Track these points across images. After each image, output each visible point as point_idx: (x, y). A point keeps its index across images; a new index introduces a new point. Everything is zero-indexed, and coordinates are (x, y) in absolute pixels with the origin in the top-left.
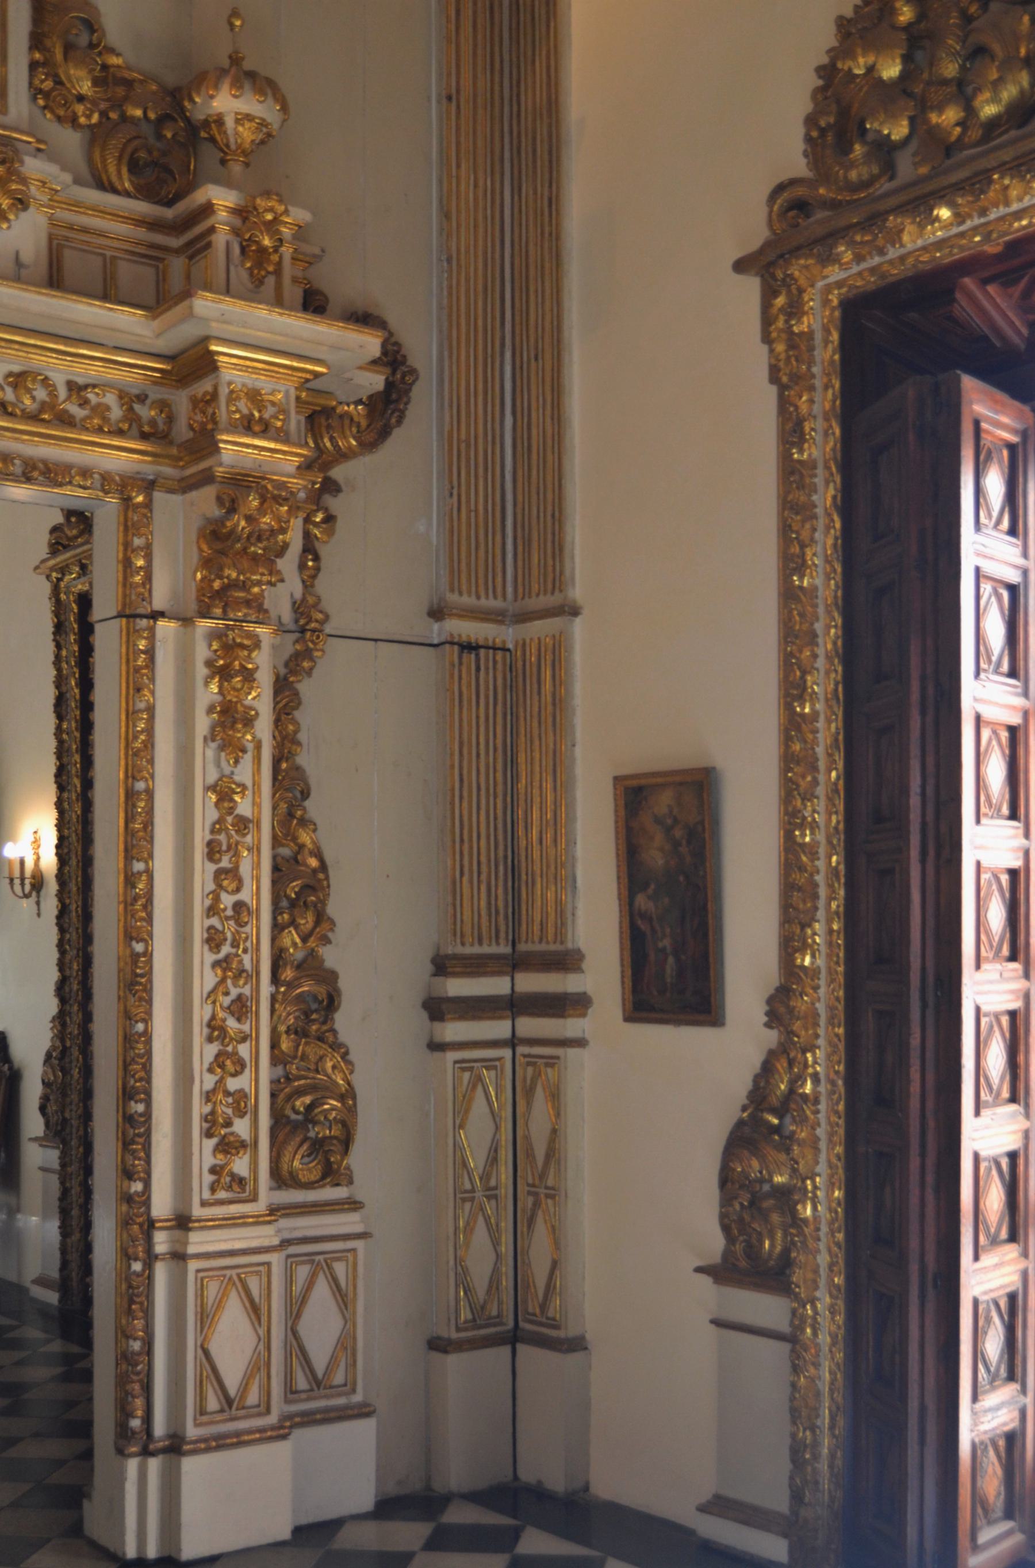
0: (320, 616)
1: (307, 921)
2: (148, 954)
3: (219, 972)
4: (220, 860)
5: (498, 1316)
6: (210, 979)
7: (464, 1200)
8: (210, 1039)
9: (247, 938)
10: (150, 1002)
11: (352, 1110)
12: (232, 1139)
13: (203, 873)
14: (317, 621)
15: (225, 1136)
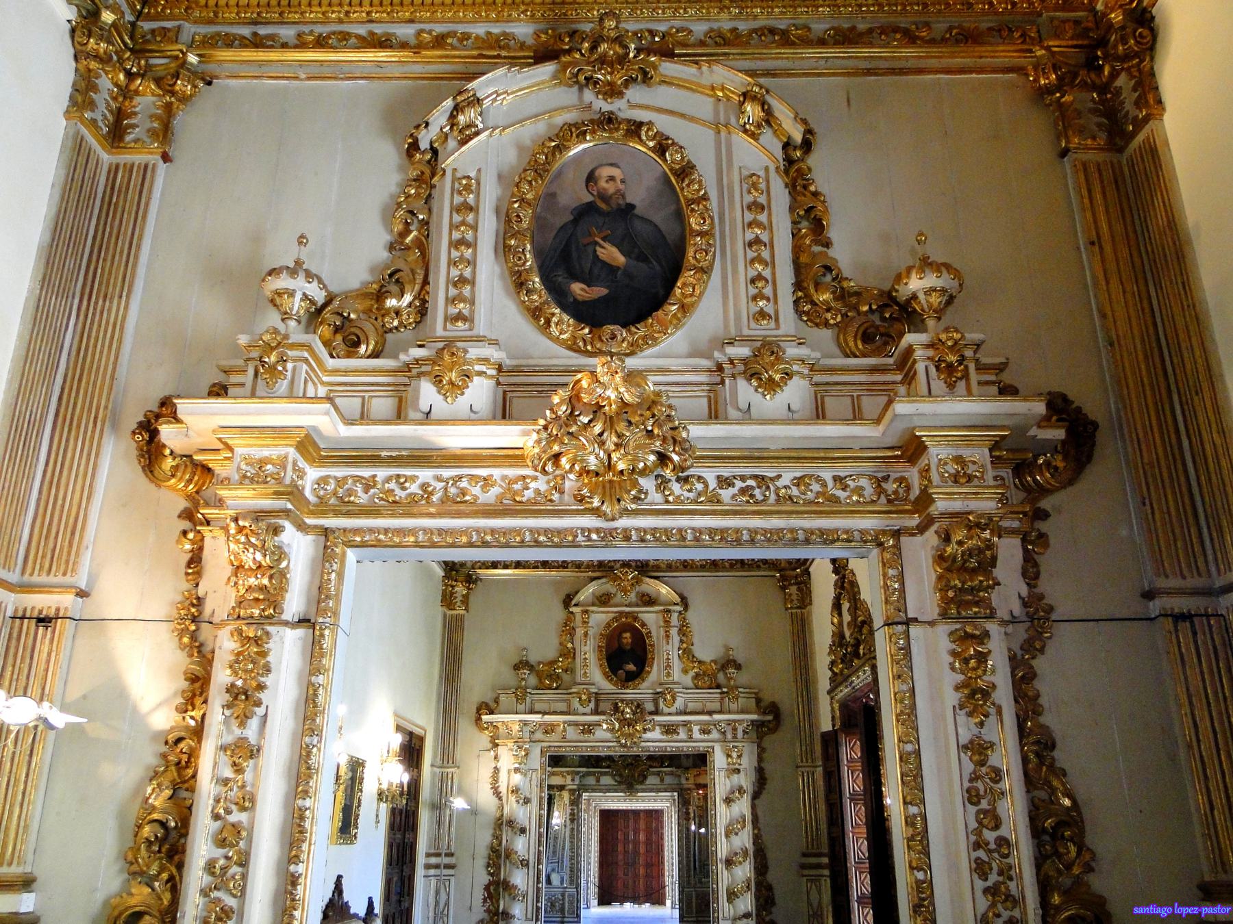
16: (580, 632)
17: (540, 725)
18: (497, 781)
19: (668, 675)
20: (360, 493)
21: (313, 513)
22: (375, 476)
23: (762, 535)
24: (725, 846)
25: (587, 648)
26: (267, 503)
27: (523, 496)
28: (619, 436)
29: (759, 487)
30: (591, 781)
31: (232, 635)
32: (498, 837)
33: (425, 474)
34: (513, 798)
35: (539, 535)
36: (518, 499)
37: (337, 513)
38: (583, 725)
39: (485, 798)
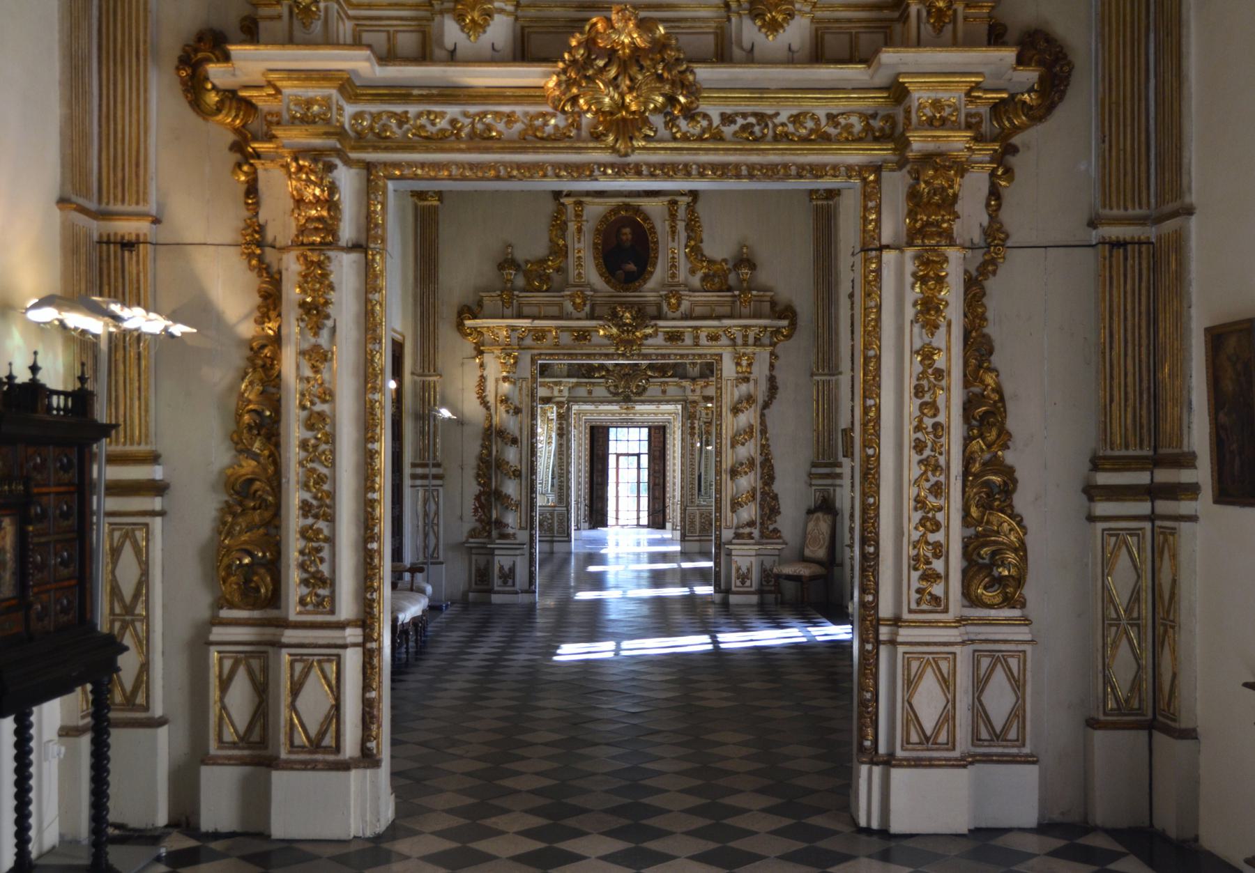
0: (1002, 236)
1: (992, 435)
2: (878, 458)
3: (923, 468)
4: (923, 396)
5: (1139, 709)
6: (917, 471)
7: (1111, 625)
8: (916, 509)
9: (942, 446)
10: (878, 486)
11: (1024, 559)
12: (930, 572)
13: (911, 407)
14: (1000, 239)
15: (925, 570)
16: (572, 226)
17: (530, 331)
18: (484, 391)
19: (673, 276)
20: (395, 129)
21: (354, 149)
22: (406, 112)
23: (759, 170)
24: (729, 457)
25: (581, 245)
26: (318, 142)
27: (544, 132)
28: (631, 80)
29: (759, 124)
30: (582, 392)
31: (298, 259)
32: (486, 446)
33: (453, 111)
34: (502, 408)
35: (560, 170)
36: (539, 134)
37: (376, 148)
38: (578, 332)
39: (472, 407)
